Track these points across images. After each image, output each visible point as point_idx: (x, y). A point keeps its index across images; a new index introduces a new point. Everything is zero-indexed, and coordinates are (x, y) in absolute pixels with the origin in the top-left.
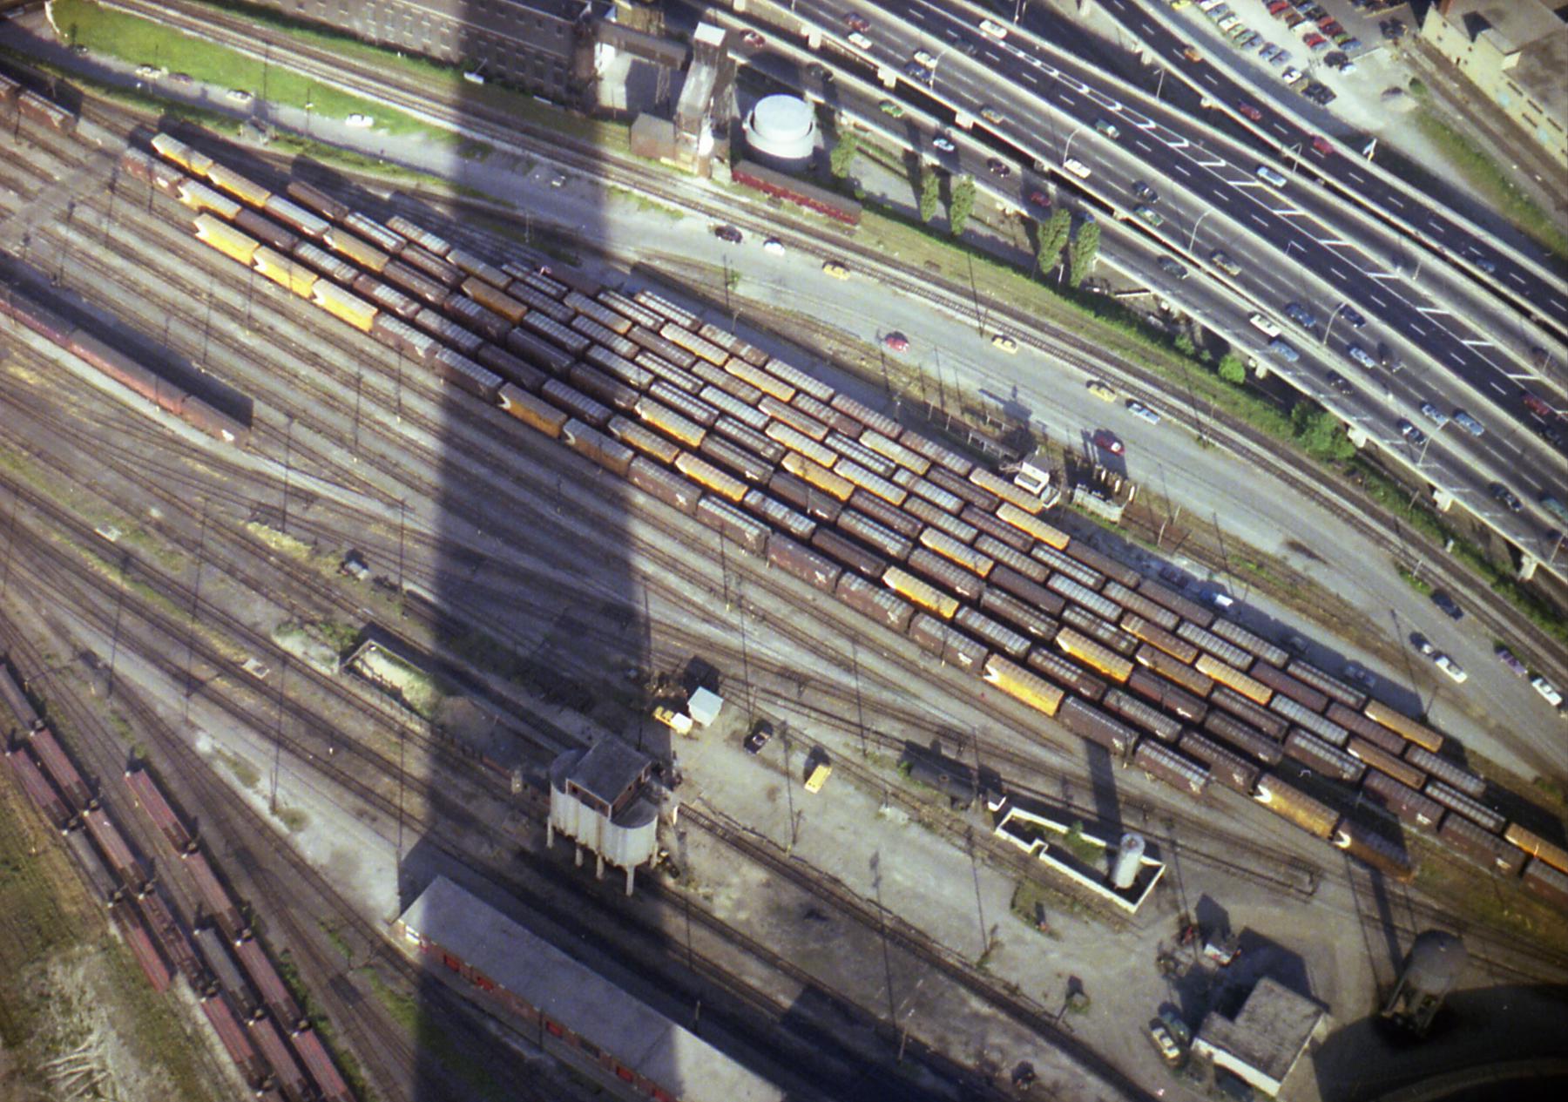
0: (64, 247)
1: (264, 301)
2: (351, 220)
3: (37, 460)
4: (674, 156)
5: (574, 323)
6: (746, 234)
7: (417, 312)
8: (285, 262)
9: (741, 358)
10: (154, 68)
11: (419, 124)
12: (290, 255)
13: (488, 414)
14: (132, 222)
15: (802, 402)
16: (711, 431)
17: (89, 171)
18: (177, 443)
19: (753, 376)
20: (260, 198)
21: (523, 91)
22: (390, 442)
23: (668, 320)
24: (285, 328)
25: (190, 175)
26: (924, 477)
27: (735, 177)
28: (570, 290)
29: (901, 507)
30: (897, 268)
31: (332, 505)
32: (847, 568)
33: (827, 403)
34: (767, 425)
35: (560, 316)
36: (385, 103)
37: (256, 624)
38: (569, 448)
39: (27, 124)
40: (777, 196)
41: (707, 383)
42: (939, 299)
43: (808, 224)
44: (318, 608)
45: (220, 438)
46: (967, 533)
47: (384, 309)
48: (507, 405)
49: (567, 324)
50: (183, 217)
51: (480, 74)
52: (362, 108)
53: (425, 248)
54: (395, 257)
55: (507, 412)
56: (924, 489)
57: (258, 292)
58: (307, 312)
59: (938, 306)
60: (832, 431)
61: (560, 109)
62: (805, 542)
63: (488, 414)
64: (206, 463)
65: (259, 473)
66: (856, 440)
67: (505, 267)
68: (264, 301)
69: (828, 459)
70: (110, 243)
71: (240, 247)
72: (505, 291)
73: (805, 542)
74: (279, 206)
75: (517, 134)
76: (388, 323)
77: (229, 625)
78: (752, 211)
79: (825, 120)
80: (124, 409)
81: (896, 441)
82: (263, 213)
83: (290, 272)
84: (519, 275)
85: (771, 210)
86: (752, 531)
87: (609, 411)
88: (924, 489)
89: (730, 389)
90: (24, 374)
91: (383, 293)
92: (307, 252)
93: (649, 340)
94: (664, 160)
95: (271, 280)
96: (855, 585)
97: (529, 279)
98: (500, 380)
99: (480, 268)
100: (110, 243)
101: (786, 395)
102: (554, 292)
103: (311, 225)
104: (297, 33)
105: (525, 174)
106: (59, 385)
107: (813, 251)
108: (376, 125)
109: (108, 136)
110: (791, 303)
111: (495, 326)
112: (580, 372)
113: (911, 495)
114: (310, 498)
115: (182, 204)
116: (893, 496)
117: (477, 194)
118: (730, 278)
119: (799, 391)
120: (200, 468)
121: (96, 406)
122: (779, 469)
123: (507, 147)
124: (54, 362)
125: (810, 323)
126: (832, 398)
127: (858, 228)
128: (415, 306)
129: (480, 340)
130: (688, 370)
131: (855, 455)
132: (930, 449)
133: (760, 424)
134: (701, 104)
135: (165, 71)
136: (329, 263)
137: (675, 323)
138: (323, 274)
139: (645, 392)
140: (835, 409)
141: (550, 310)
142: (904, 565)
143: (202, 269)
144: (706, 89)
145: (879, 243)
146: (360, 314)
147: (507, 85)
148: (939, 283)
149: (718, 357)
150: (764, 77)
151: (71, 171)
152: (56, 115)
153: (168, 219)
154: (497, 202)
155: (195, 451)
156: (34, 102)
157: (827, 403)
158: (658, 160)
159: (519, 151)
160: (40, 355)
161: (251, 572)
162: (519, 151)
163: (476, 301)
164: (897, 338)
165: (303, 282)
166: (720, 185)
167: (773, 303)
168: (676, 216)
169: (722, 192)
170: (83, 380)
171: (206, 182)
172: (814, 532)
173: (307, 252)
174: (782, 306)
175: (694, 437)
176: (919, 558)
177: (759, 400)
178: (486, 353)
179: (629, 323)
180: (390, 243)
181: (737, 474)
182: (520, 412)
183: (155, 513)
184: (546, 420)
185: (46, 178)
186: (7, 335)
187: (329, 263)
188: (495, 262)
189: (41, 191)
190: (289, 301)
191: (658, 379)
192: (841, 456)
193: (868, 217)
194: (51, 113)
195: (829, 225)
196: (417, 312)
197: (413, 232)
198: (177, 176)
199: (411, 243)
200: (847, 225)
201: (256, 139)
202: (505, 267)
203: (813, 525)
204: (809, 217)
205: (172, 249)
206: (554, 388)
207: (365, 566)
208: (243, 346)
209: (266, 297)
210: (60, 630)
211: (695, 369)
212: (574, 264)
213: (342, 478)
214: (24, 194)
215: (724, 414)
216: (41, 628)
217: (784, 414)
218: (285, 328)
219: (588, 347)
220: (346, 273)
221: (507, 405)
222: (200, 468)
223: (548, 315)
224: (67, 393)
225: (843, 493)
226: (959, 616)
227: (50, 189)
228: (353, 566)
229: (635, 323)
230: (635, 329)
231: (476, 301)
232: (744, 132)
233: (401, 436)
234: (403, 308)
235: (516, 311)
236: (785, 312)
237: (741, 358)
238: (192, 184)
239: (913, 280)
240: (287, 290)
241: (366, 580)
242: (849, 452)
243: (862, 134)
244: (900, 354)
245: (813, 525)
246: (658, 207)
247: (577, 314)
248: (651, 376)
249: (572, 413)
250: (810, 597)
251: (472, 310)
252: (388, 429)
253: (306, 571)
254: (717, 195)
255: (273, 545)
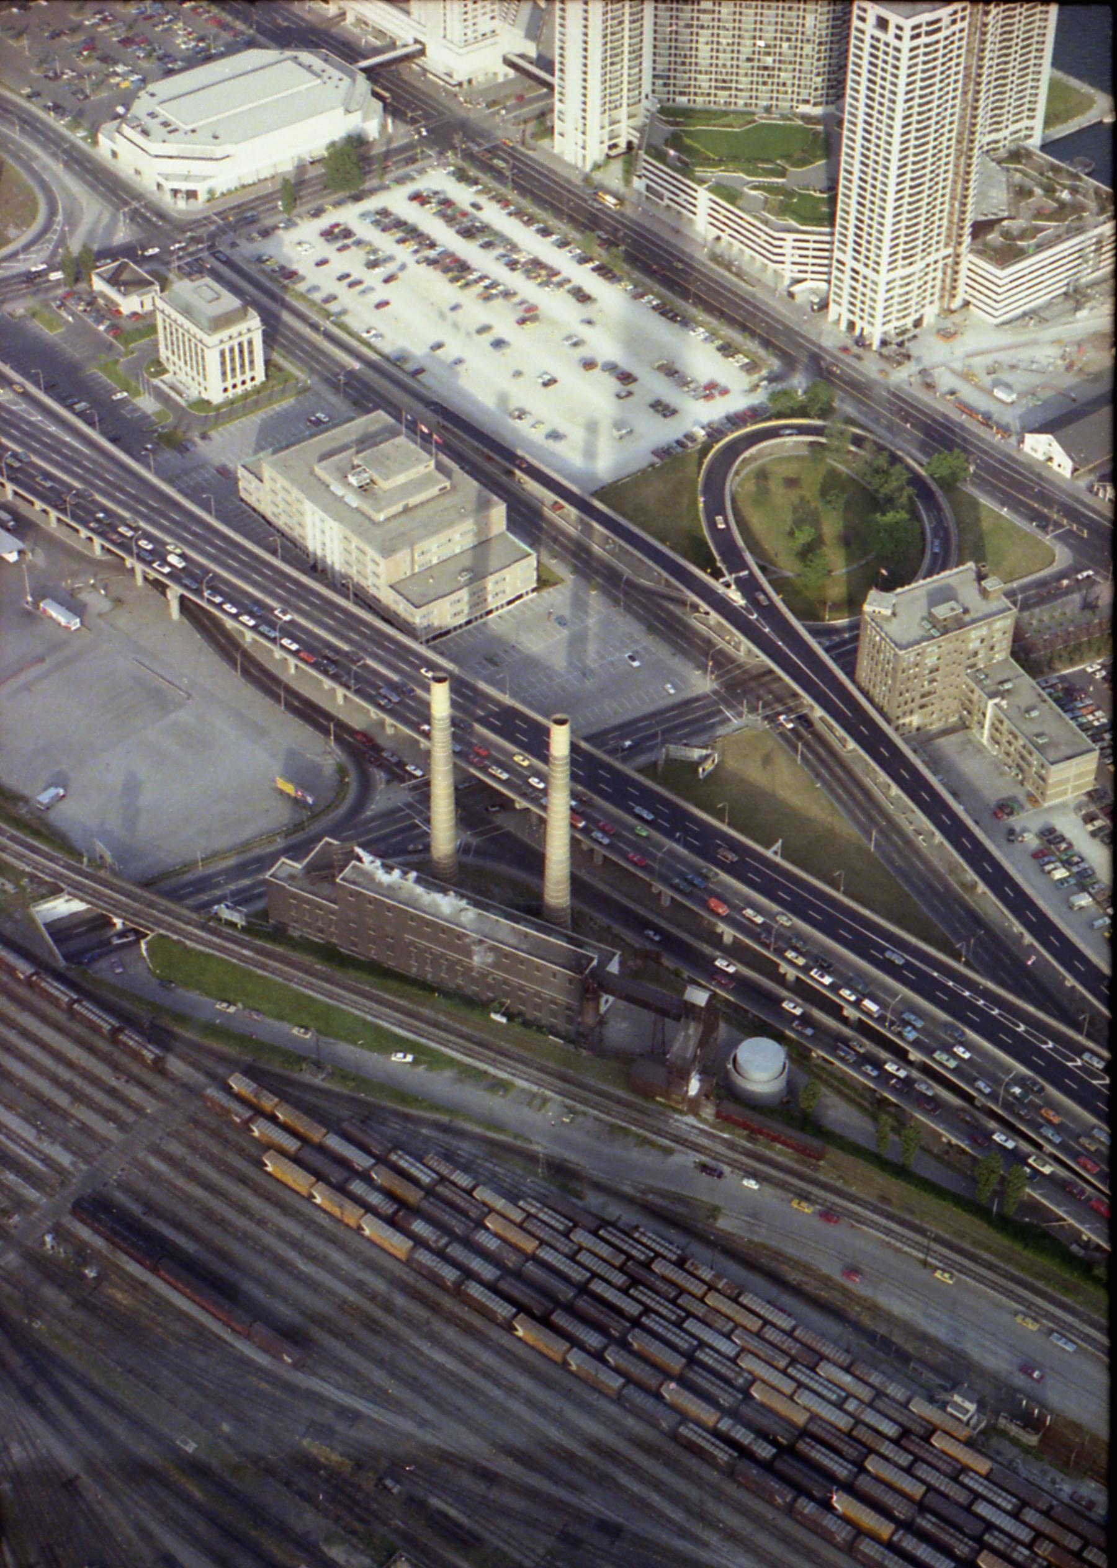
0: (154, 1177)
1: (320, 1231)
2: (394, 1157)
3: (130, 1377)
4: (667, 1096)
5: (578, 1257)
6: (727, 1169)
7: (446, 1245)
8: (338, 1197)
9: (718, 1291)
10: (230, 1003)
11: (451, 1062)
12: (341, 1189)
13: (505, 1340)
14: (212, 1155)
15: (770, 1334)
16: (691, 1360)
17: (175, 1106)
18: (245, 1362)
19: (727, 1307)
20: (317, 1134)
21: (540, 1029)
22: (421, 1365)
23: (658, 1255)
24: (337, 1257)
25: (259, 1112)
26: (870, 1405)
27: (718, 1115)
28: (576, 1225)
29: (849, 1435)
30: (853, 1202)
31: (374, 1423)
32: (801, 1491)
33: (790, 1334)
34: (738, 1355)
35: (566, 1250)
36: (423, 1041)
37: (308, 1533)
38: (571, 1373)
39: (125, 1060)
40: (753, 1133)
41: (690, 1315)
42: (888, 1232)
43: (780, 1159)
44: (360, 1519)
45: (281, 1360)
46: (904, 1459)
47: (419, 1242)
48: (520, 1333)
49: (572, 1257)
50: (253, 1151)
51: (504, 1015)
52: (405, 1046)
53: (454, 1184)
54: (429, 1192)
55: (519, 1339)
56: (870, 1417)
57: (315, 1222)
58: (356, 1243)
59: (887, 1239)
60: (793, 1361)
61: (571, 1047)
62: (767, 1466)
63: (505, 1340)
64: (268, 1382)
65: (314, 1393)
66: (813, 1369)
67: (521, 1203)
68: (320, 1231)
69: (788, 1387)
70: (192, 1175)
71: (298, 1179)
72: (520, 1226)
73: (767, 1466)
74: (334, 1142)
75: (535, 1073)
76: (425, 1258)
77: (284, 1532)
78: (731, 1145)
79: (798, 1055)
80: (201, 1330)
81: (847, 1370)
82: (321, 1149)
83: (341, 1207)
84: (533, 1211)
85: (749, 1145)
86: (723, 1455)
87: (605, 1341)
88: (870, 1417)
89: (708, 1320)
90: (120, 1296)
91: (419, 1227)
92: (357, 1187)
93: (641, 1273)
94: (658, 1099)
95: (325, 1211)
96: (808, 1507)
97: (541, 1215)
98: (514, 1310)
99: (500, 1204)
100: (192, 1175)
101: (754, 1324)
102: (561, 1228)
103: (361, 1161)
104: (351, 973)
105: (539, 1110)
106: (148, 1306)
107: (783, 1186)
108: (415, 1062)
109: (191, 1070)
110: (762, 1236)
111: (512, 1260)
112: (582, 1304)
113: (858, 1422)
114: (355, 1417)
115: (254, 1138)
116: (843, 1422)
117: (499, 1128)
118: (714, 1212)
119: (766, 1322)
120: (263, 1386)
121: (178, 1327)
122: (748, 1397)
123: (525, 1084)
124: (144, 1285)
125: (778, 1255)
126: (794, 1328)
127: (822, 1163)
128: (444, 1241)
129: (498, 1273)
130: (673, 1302)
131: (812, 1384)
132: (875, 1378)
133: (732, 1354)
134: (689, 1054)
135: (240, 1005)
136: (375, 1199)
137: (664, 1257)
138: (369, 1209)
139: (636, 1323)
140: (796, 1340)
141: (558, 1245)
142: (850, 1489)
143: (268, 1199)
144: (692, 1043)
145: (840, 1177)
146: (399, 1244)
147: (527, 1024)
148: (889, 1217)
149: (698, 1289)
150: (746, 1011)
151: (161, 1105)
152: (149, 1053)
153: (241, 1152)
154: (516, 1136)
155: (259, 1370)
156: (131, 1039)
157: (790, 1334)
158: (653, 1099)
159: (535, 1088)
160: (132, 1278)
161: (304, 1486)
162: (535, 1088)
163: (496, 1235)
164: (852, 1271)
165: (352, 1215)
166: (705, 1121)
167: (747, 1236)
168: (668, 1152)
169: (706, 1128)
170: (169, 1303)
171: (272, 1119)
172: (775, 1457)
173: (357, 1187)
174: (756, 1239)
175: (676, 1364)
176: (863, 1482)
177: (732, 1331)
178: (504, 1286)
179: (623, 1257)
180: (426, 1179)
181: (710, 1400)
182: (530, 1340)
183: (226, 1428)
184: (555, 1347)
185: (139, 1110)
186: (108, 1260)
187: (375, 1199)
188: (513, 1198)
189: (135, 1122)
190: (340, 1232)
191: (647, 1310)
192: (800, 1385)
193: (834, 1154)
194: (145, 1052)
195: (797, 1161)
196: (446, 1245)
197: (444, 1169)
198: (248, 1114)
199: (443, 1179)
200: (814, 1161)
201: (315, 1076)
202: (521, 1203)
203: (774, 1450)
204: (780, 1153)
205: (243, 1180)
206: (559, 1318)
207: (397, 1482)
208: (301, 1272)
209: (322, 1227)
210: (146, 1536)
211: (680, 1301)
212: (580, 1198)
213: (380, 1397)
214: (122, 1126)
215: (702, 1344)
216: (131, 1533)
217: (754, 1344)
218: (337, 1257)
219: (589, 1281)
220: (388, 1208)
221: (520, 1333)
222: (263, 1386)
223: (556, 1249)
224: (154, 1314)
225: (800, 1418)
226: (895, 1538)
227: (143, 1121)
228: (389, 1483)
229: (630, 1257)
230: (630, 1263)
231: (496, 1235)
232: (727, 1071)
233: (430, 1359)
234: (436, 1241)
235: (529, 1245)
236: (757, 1244)
237: (718, 1291)
238: (261, 1121)
239: (868, 1214)
240: (340, 1221)
241: (400, 1493)
242: (806, 1380)
243: (828, 1067)
244: (857, 1285)
245: (774, 1450)
246: (652, 1144)
247: (581, 1249)
248: (641, 1308)
249: (575, 1342)
250: (770, 1517)
251: (492, 1244)
252: (422, 1354)
253: (352, 1485)
254: (702, 1131)
255: (323, 1460)
